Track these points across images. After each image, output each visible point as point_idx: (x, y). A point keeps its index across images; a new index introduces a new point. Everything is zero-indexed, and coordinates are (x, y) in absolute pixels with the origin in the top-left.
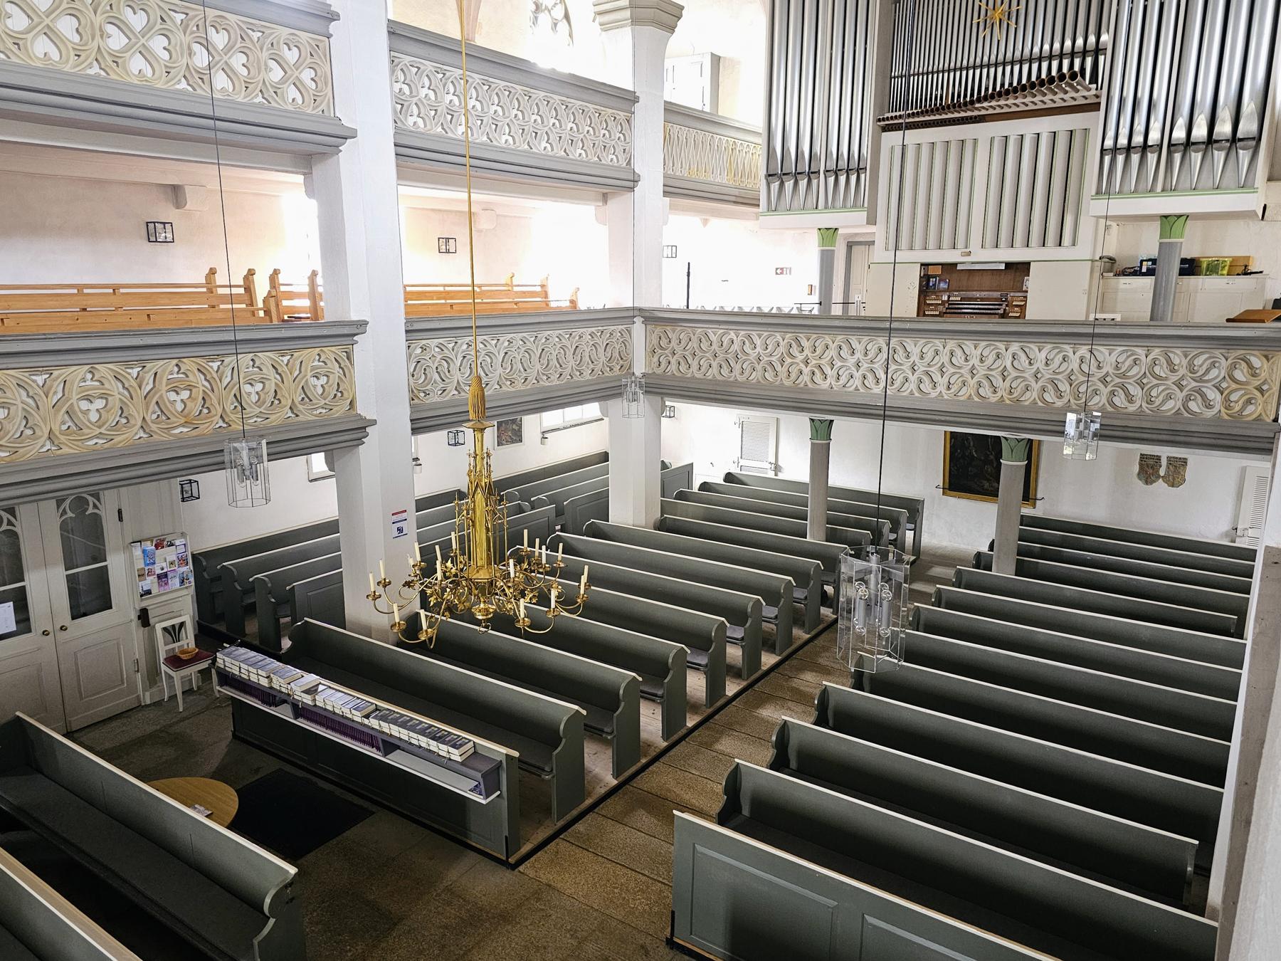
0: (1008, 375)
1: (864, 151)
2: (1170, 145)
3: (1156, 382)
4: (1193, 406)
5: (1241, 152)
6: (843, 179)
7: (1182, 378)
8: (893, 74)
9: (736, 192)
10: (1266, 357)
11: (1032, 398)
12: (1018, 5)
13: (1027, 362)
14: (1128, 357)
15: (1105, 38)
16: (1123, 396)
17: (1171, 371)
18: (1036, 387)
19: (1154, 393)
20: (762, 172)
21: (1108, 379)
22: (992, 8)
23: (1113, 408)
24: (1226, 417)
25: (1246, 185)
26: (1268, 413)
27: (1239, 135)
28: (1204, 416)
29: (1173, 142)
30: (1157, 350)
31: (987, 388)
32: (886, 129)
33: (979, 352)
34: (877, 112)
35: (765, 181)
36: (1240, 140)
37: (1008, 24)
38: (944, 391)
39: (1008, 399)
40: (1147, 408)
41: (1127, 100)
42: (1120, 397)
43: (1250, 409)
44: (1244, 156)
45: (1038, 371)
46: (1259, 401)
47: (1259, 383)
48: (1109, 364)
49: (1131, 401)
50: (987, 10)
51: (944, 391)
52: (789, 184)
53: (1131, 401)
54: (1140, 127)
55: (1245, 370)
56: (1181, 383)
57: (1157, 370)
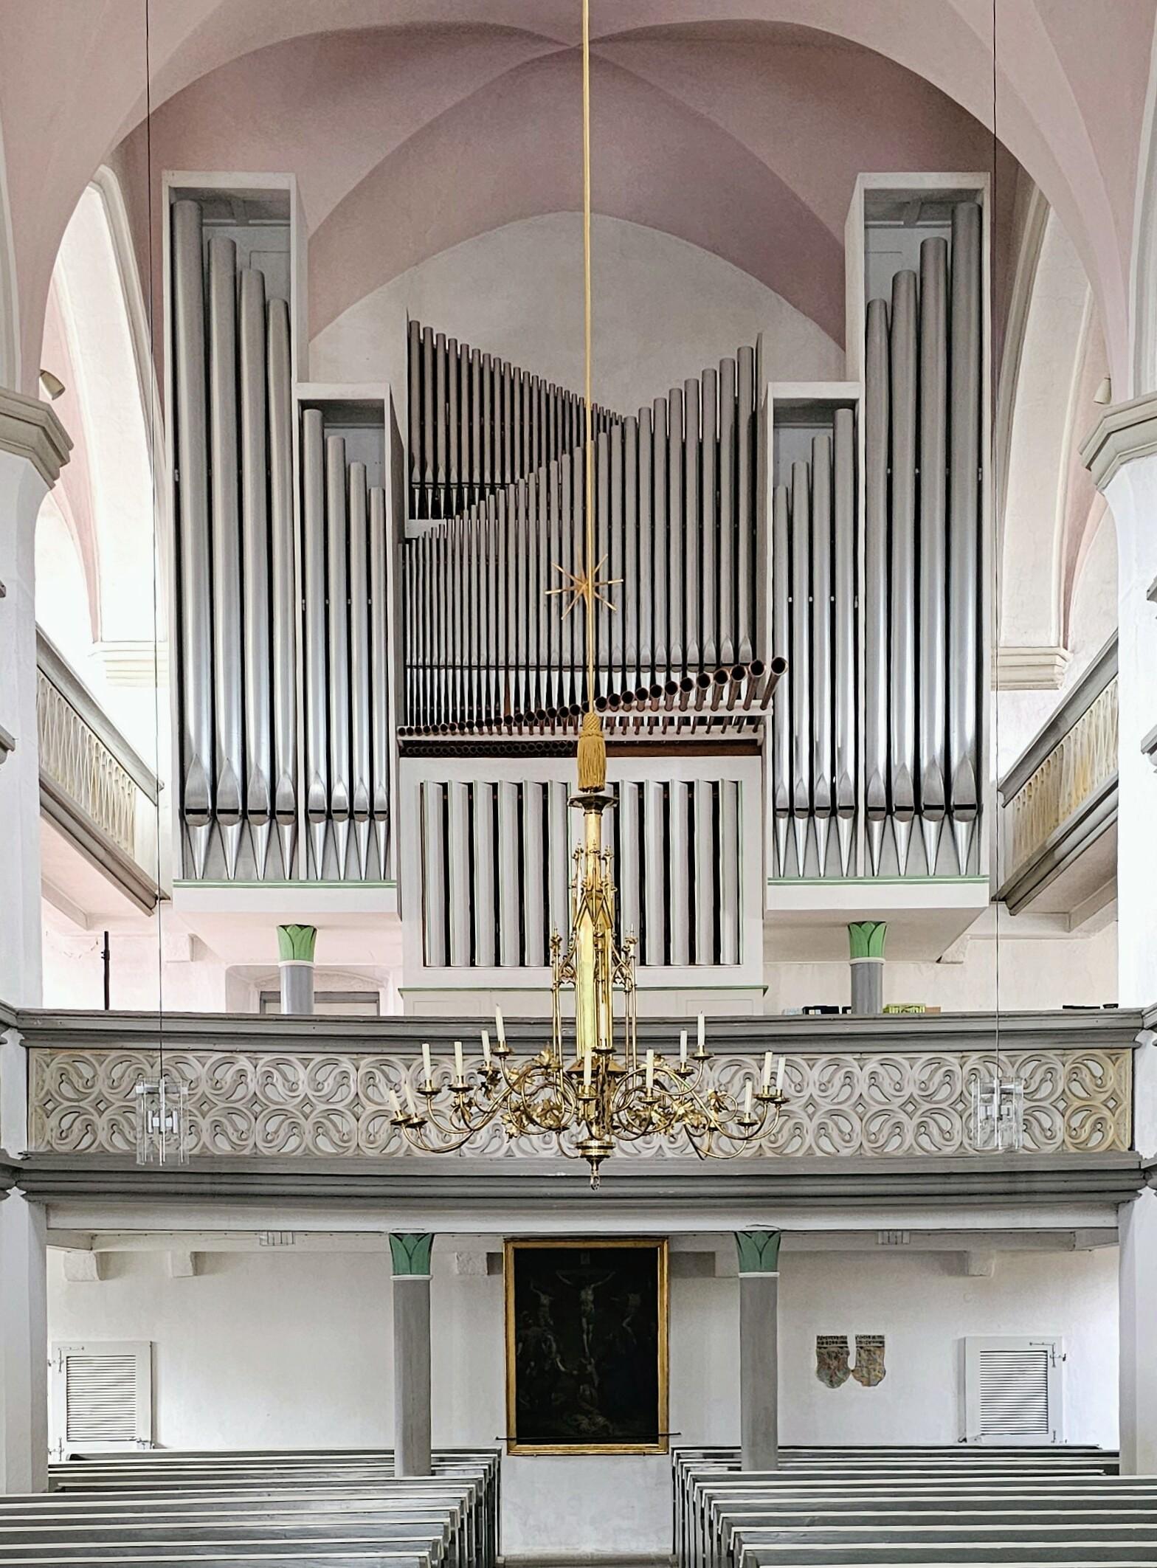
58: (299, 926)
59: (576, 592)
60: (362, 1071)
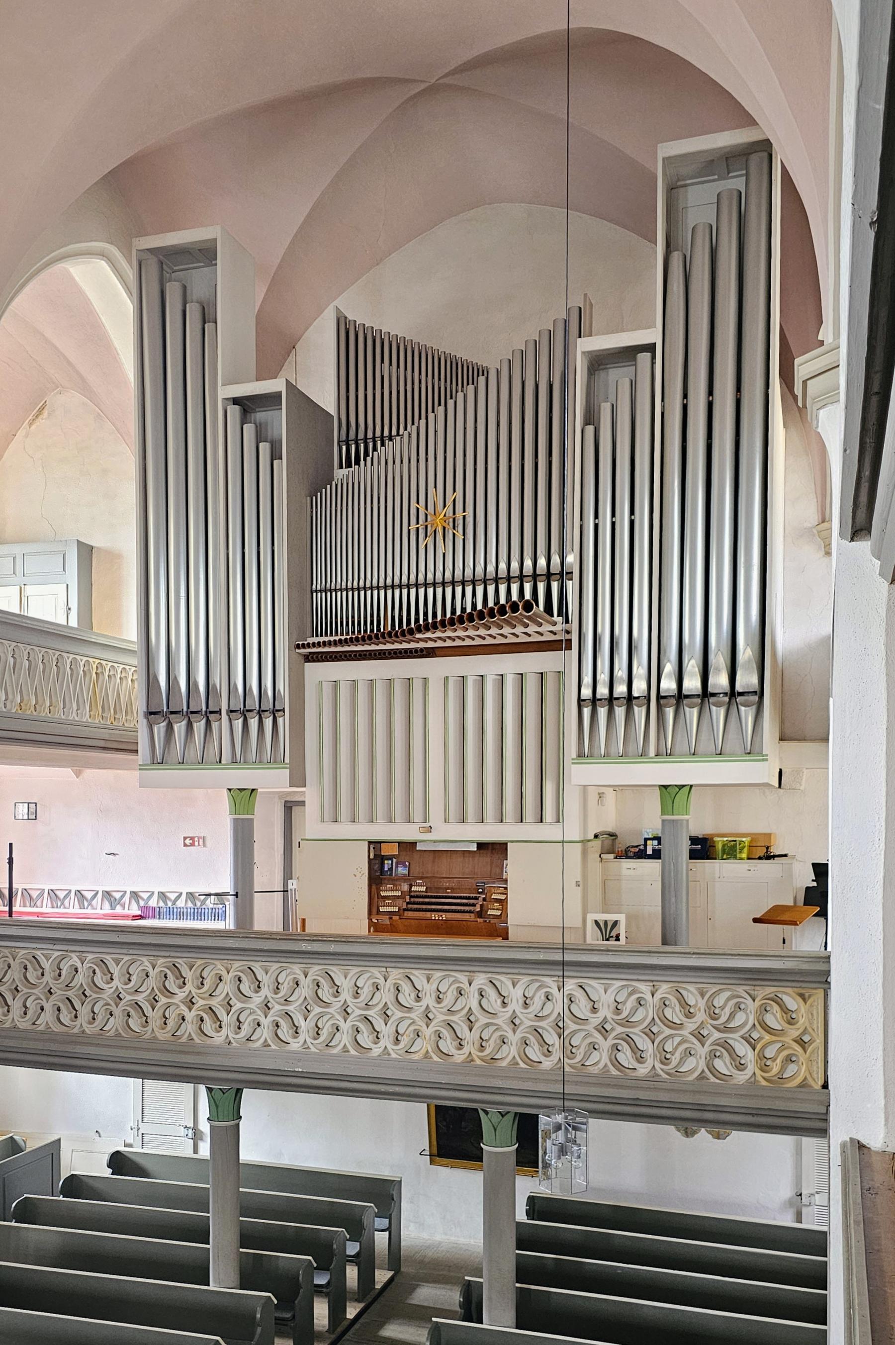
0: (476, 1021)
1: (280, 686)
2: (659, 697)
3: (668, 1032)
4: (719, 1064)
5: (742, 709)
6: (254, 723)
7: (702, 1025)
8: (314, 587)
9: (105, 735)
10: (802, 996)
11: (510, 1057)
12: (464, 511)
13: (499, 1001)
14: (630, 994)
15: (571, 559)
16: (629, 1052)
17: (687, 1017)
18: (514, 1039)
19: (669, 1047)
20: (140, 705)
21: (608, 1027)
22: (433, 513)
23: (618, 1070)
24: (764, 1083)
25: (753, 752)
26: (815, 1076)
27: (738, 688)
28: (735, 1081)
29: (662, 694)
30: (665, 987)
31: (449, 1041)
32: (311, 658)
33: (434, 987)
34: (295, 637)
35: (145, 721)
36: (741, 694)
37: (454, 534)
38: (390, 1047)
39: (478, 1056)
40: (662, 1070)
41: (602, 639)
42: (625, 1054)
43: (792, 1069)
44: (748, 714)
45: (514, 1016)
46: (802, 1059)
47: (797, 1033)
48: (606, 1006)
49: (641, 1060)
50: (426, 515)
51: (390, 1047)
52: (179, 727)
53: (641, 1060)
54: (621, 673)
55: (778, 1015)
56: (701, 1032)
57: (668, 1013)
58: (239, 789)
59: (429, 526)
60: (157, 970)
